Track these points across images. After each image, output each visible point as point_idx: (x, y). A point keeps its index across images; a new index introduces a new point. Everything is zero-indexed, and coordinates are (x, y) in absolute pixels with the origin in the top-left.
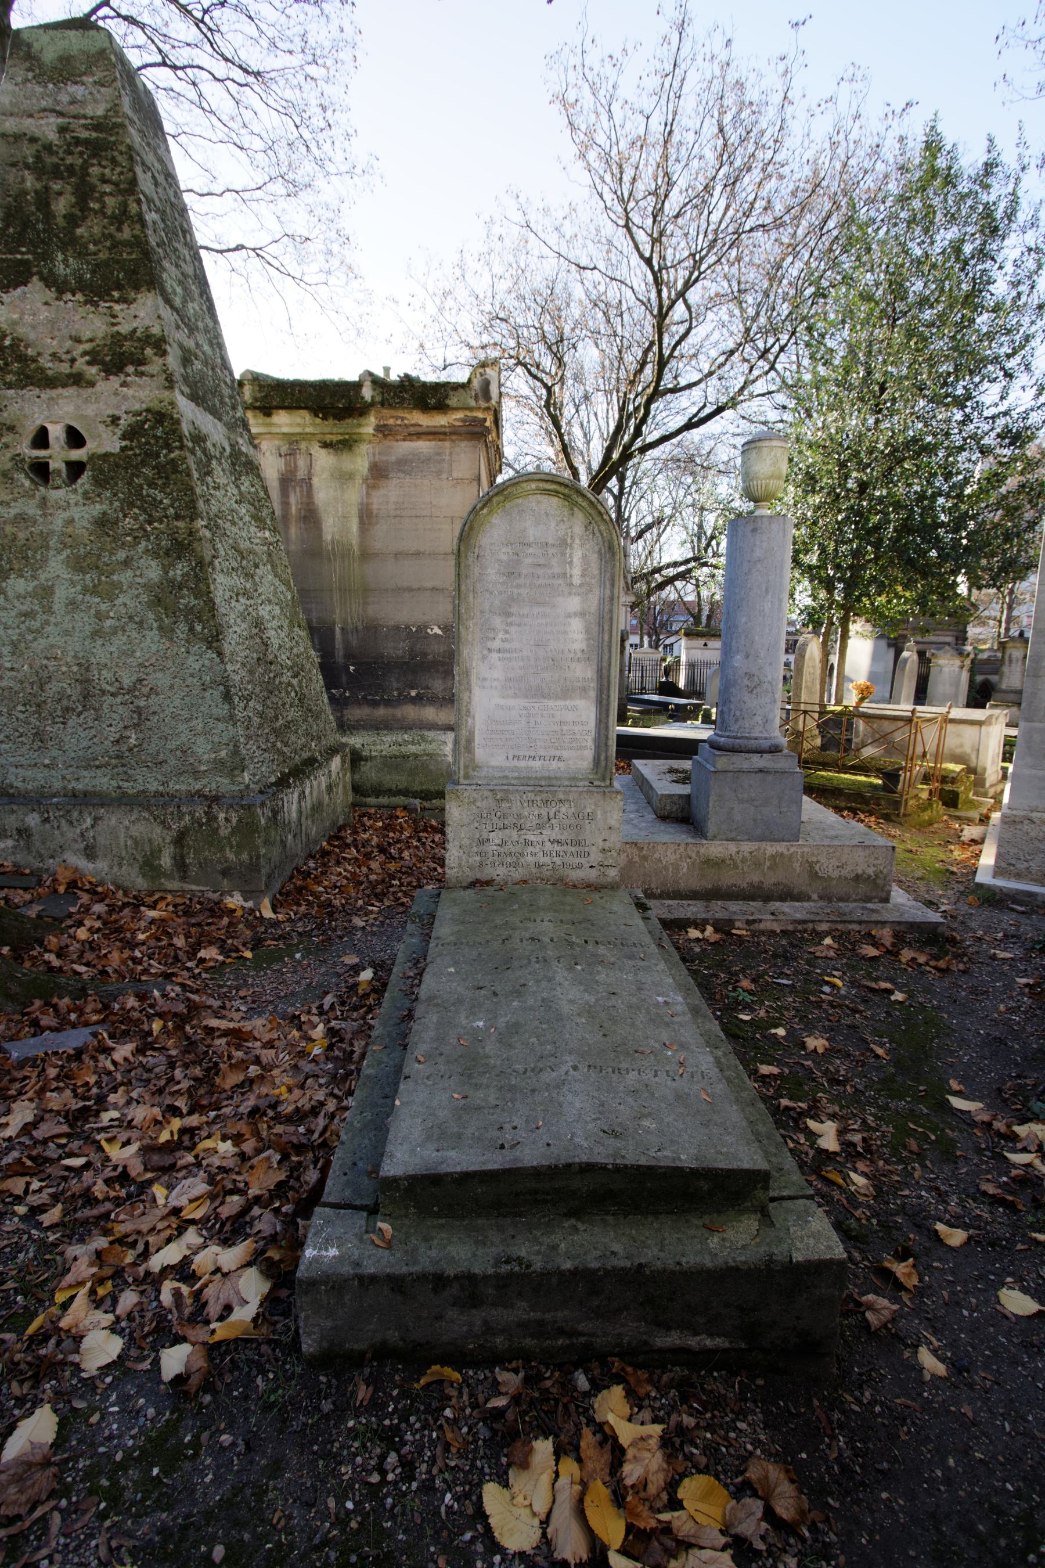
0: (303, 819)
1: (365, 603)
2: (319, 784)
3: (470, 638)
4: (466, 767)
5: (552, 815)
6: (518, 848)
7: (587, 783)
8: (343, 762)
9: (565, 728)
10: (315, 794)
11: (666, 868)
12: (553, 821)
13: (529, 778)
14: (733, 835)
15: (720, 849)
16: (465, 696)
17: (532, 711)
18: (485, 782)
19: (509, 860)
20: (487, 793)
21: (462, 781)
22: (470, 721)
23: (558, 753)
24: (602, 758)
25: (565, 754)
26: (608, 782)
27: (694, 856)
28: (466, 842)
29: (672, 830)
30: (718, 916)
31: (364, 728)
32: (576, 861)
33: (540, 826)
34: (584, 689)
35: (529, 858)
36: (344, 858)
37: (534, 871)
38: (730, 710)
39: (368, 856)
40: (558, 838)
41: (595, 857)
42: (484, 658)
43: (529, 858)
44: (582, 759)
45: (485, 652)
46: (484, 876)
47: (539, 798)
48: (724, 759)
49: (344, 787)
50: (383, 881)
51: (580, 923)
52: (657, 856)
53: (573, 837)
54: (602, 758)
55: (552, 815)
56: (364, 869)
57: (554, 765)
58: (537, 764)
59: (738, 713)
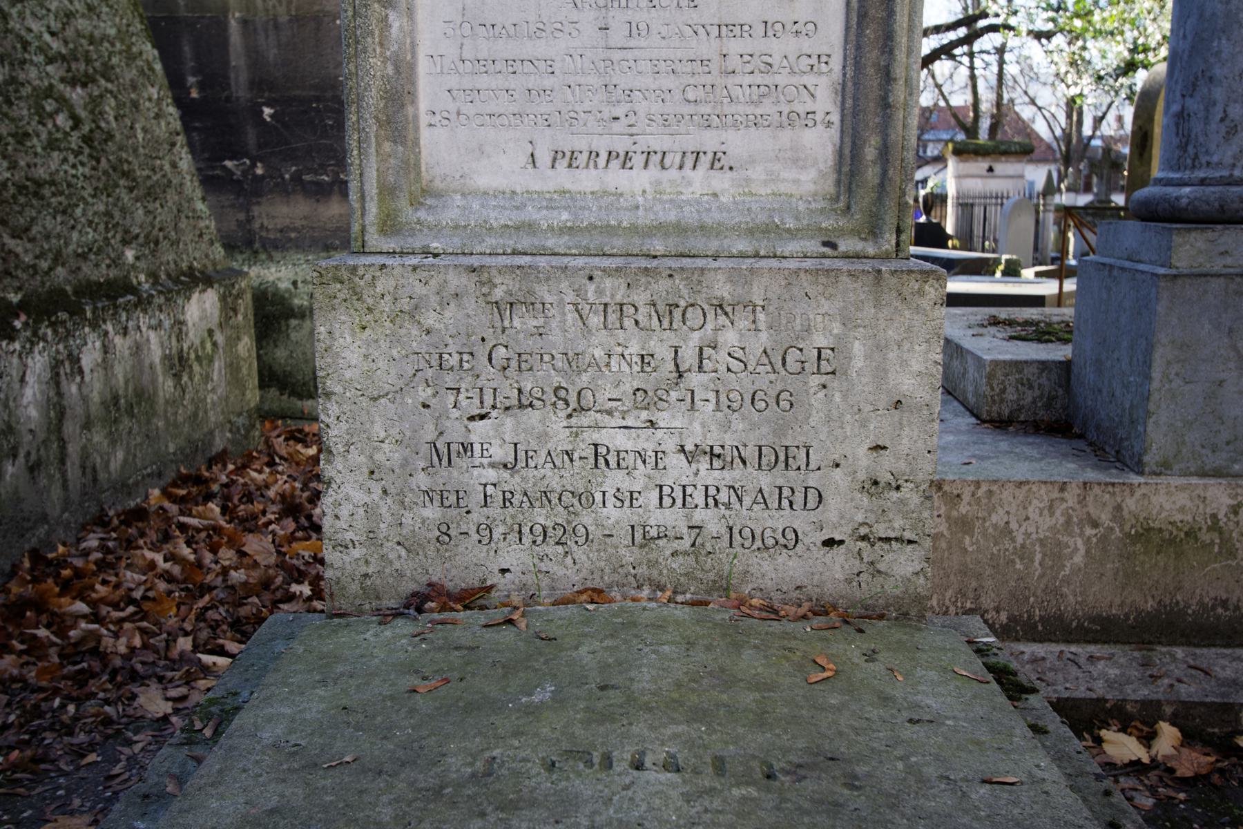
2: (137, 350)
4: (388, 192)
5: (689, 357)
7: (814, 246)
8: (228, 307)
9: (735, 47)
10: (120, 372)
11: (1024, 553)
12: (694, 379)
13: (610, 230)
14: (1219, 460)
15: (1182, 499)
18: (455, 243)
19: (541, 517)
20: (457, 281)
21: (374, 240)
22: (396, 22)
23: (710, 141)
24: (870, 153)
25: (737, 143)
27: (1105, 518)
28: (389, 454)
30: (1189, 691)
31: (298, 246)
32: (778, 520)
33: (645, 398)
35: (612, 512)
36: (183, 527)
37: (629, 556)
38: (1210, 104)
39: (250, 524)
41: (843, 508)
43: (612, 512)
46: (456, 577)
47: (641, 297)
49: (233, 367)
50: (266, 584)
51: (797, 772)
52: (998, 518)
53: (763, 435)
54: (870, 153)
55: (689, 357)
57: (699, 181)
58: (636, 182)
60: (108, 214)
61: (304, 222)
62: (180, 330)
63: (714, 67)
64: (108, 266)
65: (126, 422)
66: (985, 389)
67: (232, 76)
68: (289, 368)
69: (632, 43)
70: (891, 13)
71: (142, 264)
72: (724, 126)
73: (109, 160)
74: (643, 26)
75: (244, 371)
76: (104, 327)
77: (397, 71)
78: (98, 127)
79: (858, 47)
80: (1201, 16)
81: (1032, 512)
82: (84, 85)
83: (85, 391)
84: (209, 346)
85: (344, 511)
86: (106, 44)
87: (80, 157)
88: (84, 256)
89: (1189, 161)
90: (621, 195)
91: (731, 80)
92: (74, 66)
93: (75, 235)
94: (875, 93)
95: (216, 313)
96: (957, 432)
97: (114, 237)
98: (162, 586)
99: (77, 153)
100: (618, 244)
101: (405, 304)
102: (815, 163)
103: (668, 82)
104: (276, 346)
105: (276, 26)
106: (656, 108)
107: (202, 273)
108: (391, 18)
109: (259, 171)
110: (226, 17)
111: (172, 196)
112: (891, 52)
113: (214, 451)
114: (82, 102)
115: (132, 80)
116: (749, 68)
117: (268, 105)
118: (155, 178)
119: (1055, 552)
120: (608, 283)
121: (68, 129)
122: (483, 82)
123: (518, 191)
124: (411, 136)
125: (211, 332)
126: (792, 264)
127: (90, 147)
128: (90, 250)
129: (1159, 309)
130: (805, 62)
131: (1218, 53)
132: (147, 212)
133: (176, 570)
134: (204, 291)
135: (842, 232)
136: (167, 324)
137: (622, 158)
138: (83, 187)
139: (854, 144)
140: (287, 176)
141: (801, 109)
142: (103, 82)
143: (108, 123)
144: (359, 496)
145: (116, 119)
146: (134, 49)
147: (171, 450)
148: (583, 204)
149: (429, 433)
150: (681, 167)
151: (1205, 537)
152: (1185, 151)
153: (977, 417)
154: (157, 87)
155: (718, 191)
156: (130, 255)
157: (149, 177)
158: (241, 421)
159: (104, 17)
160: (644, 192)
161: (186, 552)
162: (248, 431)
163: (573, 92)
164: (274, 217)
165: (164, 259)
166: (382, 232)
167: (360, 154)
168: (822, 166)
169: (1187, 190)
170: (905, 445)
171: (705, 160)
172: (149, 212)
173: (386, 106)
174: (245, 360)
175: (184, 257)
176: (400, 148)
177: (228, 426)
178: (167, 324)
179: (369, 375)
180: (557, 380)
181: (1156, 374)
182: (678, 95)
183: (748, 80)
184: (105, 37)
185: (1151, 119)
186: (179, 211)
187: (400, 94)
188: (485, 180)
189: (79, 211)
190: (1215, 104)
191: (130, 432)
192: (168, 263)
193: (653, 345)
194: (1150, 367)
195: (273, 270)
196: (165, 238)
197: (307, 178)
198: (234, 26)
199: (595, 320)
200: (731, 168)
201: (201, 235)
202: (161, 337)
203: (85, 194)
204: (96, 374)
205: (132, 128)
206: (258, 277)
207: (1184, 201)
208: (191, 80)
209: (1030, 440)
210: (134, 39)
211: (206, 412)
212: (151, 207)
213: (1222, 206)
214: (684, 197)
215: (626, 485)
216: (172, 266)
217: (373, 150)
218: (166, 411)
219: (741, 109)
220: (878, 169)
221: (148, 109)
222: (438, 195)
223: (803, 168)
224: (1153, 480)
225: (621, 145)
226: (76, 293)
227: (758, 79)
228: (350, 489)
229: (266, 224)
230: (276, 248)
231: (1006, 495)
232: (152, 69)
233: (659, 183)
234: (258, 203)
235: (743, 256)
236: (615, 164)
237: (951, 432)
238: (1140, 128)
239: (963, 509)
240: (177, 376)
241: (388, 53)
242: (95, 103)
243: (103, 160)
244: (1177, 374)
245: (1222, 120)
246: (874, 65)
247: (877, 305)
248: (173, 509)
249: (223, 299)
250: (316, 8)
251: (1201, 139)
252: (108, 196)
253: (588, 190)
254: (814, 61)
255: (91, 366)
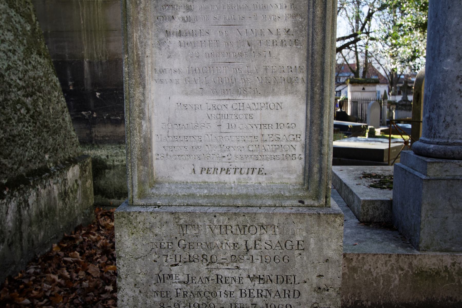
0: (24, 227)
1: (108, 41)
2: (49, 193)
3: (141, 16)
4: (142, 183)
5: (251, 244)
6: (209, 286)
7: (296, 202)
8: (83, 170)
9: (266, 132)
10: (42, 202)
11: (376, 280)
12: (253, 252)
15: (434, 260)
16: (138, 93)
17: (225, 112)
18: (165, 202)
20: (166, 217)
21: (136, 200)
22: (145, 125)
23: (258, 164)
24: (315, 169)
25: (267, 165)
26: (323, 201)
27: (406, 267)
28: (142, 278)
29: (378, 238)
33: (235, 259)
34: (290, 81)
35: (223, 299)
36: (65, 262)
38: (439, 116)
39: (90, 259)
40: (260, 273)
42: (161, 43)
43: (223, 299)
44: (289, 171)
45: (162, 36)
47: (233, 223)
48: (437, 167)
49: (85, 192)
50: (96, 287)
52: (366, 267)
53: (278, 271)
54: (315, 169)
55: (251, 244)
56: (82, 274)
57: (254, 179)
58: (231, 178)
59: (448, 119)
60: (39, 143)
61: (111, 134)
62: (65, 182)
63: (259, 139)
64: (39, 163)
65: (45, 220)
66: (361, 210)
67: (85, 81)
68: (105, 188)
69: (229, 131)
70: (322, 122)
71: (52, 160)
72: (263, 159)
73: (40, 123)
74: (233, 125)
75: (89, 193)
76: (37, 187)
77: (145, 141)
78: (36, 111)
79: (311, 133)
80: (435, 84)
81: (379, 265)
82: (31, 96)
83: (30, 212)
84: (76, 186)
85: (125, 299)
86: (39, 79)
87: (30, 124)
88: (30, 161)
89: (432, 135)
90: (226, 183)
91: (265, 144)
92: (27, 90)
93: (27, 153)
94: (317, 149)
95: (78, 173)
96: (351, 228)
97: (41, 151)
98: (57, 289)
99: (28, 122)
100: (225, 202)
101: (148, 225)
102: (296, 172)
103: (243, 144)
104: (100, 179)
105: (101, 64)
106: (238, 153)
107: (73, 158)
108: (143, 123)
109: (95, 116)
110: (83, 61)
111: (63, 132)
112: (322, 135)
113: (77, 224)
114: (30, 102)
115: (49, 91)
116: (272, 139)
117: (98, 92)
118: (56, 126)
119: (388, 280)
120: (221, 218)
121: (25, 114)
122: (176, 144)
123: (189, 182)
124: (150, 163)
125: (76, 181)
126: (288, 211)
127: (33, 119)
128: (32, 158)
129: (423, 191)
130: (291, 137)
131: (442, 98)
132: (54, 139)
133: (63, 282)
134: (74, 166)
135: (306, 197)
136: (60, 181)
137: (226, 170)
138: (30, 135)
139: (310, 166)
140: (105, 117)
141: (290, 153)
142: (38, 93)
143: (40, 108)
144: (131, 293)
145: (43, 106)
146: (50, 79)
147: (61, 227)
148: (212, 187)
149: (157, 271)
150: (247, 174)
151: (443, 274)
152: (431, 131)
153: (359, 220)
154: (58, 91)
155: (261, 181)
156: (47, 157)
157: (54, 126)
158: (87, 211)
159: (39, 69)
160: (234, 182)
161: (66, 273)
162: (90, 214)
163: (208, 148)
164: (100, 132)
165: (59, 156)
166: (140, 198)
167: (131, 171)
168: (298, 173)
169: (432, 146)
170: (330, 275)
171: (256, 171)
172: (54, 139)
173: (141, 153)
174: (89, 188)
175: (67, 154)
176: (146, 168)
177: (83, 214)
178: (60, 181)
179: (135, 250)
180: (203, 252)
181: (423, 215)
182: (246, 149)
183: (271, 143)
184: (39, 77)
185: (420, 89)
186: (65, 137)
187: (146, 149)
188: (177, 178)
189: (28, 144)
190: (441, 116)
191: (46, 224)
192: (61, 157)
193: (238, 240)
194: (421, 212)
195: (99, 151)
196: (60, 148)
197: (112, 118)
198: (86, 63)
199: (217, 231)
200: (265, 174)
201: (73, 144)
202: (58, 186)
203: (31, 137)
204: (34, 205)
205: (48, 109)
206: (94, 154)
207: (431, 150)
208: (70, 83)
209: (378, 232)
210: (50, 75)
211: (74, 211)
212: (55, 137)
213: (445, 153)
214: (248, 184)
215: (229, 289)
216: (62, 158)
217: (136, 169)
218: (59, 213)
219: (269, 153)
220: (318, 175)
221: (54, 100)
222: (160, 183)
223: (292, 174)
224: (423, 253)
225: (226, 166)
226: (27, 175)
227: (275, 143)
228: (127, 291)
229: (97, 134)
230: (101, 143)
231: (369, 259)
232: (56, 85)
233: (239, 179)
234: (94, 127)
235: (270, 206)
236: (224, 172)
237: (349, 227)
238: (417, 92)
239: (354, 264)
240: (64, 200)
241: (142, 135)
242: (35, 103)
243: (38, 123)
244: (431, 215)
245: (444, 122)
246: (316, 139)
247: (319, 225)
248: (62, 254)
249: (81, 168)
250: (116, 57)
251: (437, 128)
252: (39, 136)
253: (214, 181)
254: (295, 137)
255: (32, 202)
